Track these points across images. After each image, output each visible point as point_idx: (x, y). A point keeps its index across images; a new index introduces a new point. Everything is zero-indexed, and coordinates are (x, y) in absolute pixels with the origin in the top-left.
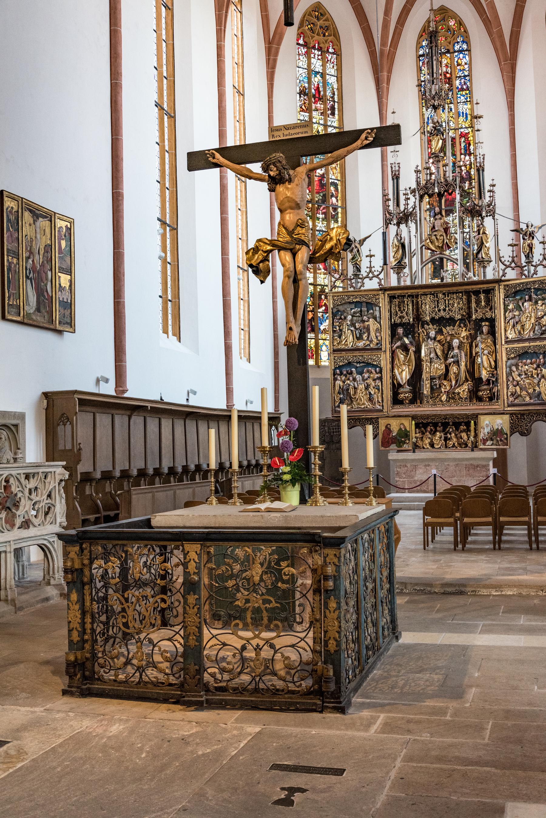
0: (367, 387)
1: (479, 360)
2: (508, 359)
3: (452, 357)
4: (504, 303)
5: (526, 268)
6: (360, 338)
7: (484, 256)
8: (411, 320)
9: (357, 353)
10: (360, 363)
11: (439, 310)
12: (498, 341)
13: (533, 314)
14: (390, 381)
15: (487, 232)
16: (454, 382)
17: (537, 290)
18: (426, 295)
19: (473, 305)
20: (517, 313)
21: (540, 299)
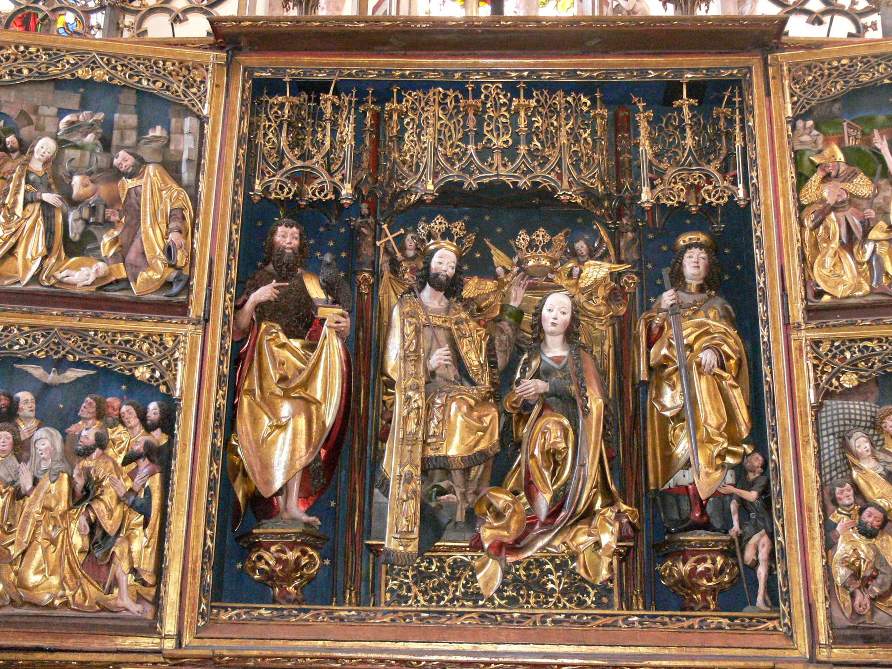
0: (85, 495)
1: (671, 399)
2: (828, 395)
3: (537, 375)
6: (78, 247)
8: (347, 190)
9: (55, 318)
10: (61, 365)
11: (485, 153)
12: (769, 310)
14: (207, 470)
16: (544, 500)
18: (426, 86)
19: (645, 148)
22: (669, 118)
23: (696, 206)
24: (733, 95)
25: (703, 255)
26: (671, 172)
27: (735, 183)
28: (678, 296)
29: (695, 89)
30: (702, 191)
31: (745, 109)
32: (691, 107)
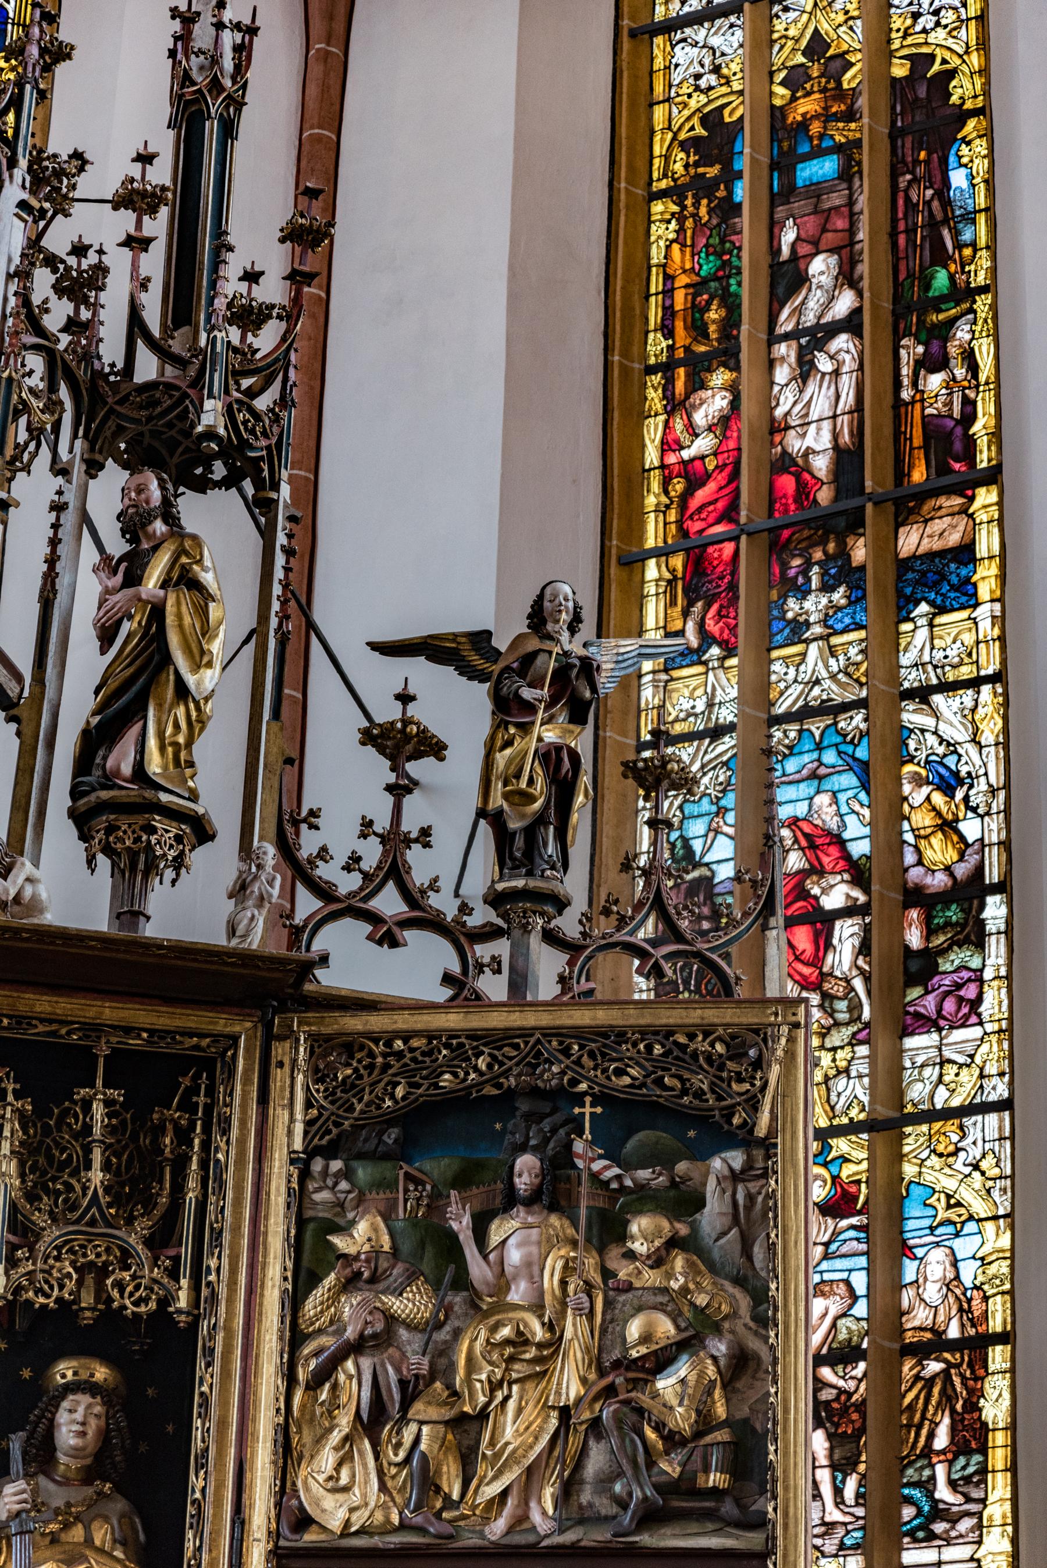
4: (299, 1198)
5: (502, 948)
7: (155, 765)
13: (572, 1327)
15: (208, 578)
17: (624, 1115)
20: (411, 1303)
21: (643, 1199)
22: (66, 1112)
23: (93, 1309)
24: (194, 1090)
25: (98, 1409)
26: (52, 1235)
27: (174, 1274)
28: (35, 1492)
29: (123, 1068)
30: (109, 1282)
31: (216, 1122)
32: (108, 1103)
